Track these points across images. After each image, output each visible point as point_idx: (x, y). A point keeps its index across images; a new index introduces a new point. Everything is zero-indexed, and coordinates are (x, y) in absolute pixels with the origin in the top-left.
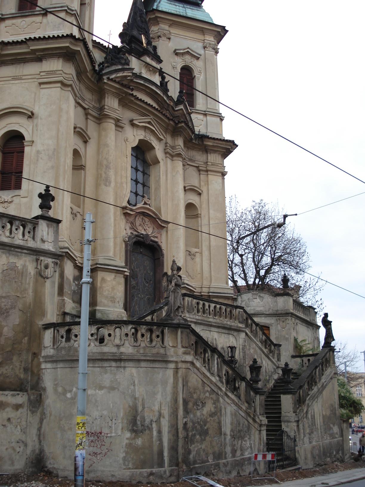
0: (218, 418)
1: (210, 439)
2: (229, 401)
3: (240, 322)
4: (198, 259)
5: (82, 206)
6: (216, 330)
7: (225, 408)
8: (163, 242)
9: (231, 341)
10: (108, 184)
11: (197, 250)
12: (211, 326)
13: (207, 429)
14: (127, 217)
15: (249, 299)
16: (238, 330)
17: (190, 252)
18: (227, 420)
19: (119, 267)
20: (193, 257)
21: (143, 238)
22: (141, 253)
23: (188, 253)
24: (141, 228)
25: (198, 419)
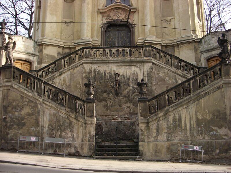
0: (36, 117)
1: (27, 128)
2: (48, 107)
3: (145, 56)
4: (172, 23)
5: (74, 18)
6: (116, 64)
7: (44, 112)
8: (135, 19)
9: (133, 71)
10: (84, 2)
11: (172, 17)
12: (109, 63)
13: (24, 122)
14: (103, 14)
15: (209, 39)
16: (143, 62)
17: (166, 20)
18: (45, 119)
19: (86, 42)
20: (169, 22)
21: (114, 22)
22: (118, 30)
23: (165, 21)
24: (115, 17)
25: (16, 116)
